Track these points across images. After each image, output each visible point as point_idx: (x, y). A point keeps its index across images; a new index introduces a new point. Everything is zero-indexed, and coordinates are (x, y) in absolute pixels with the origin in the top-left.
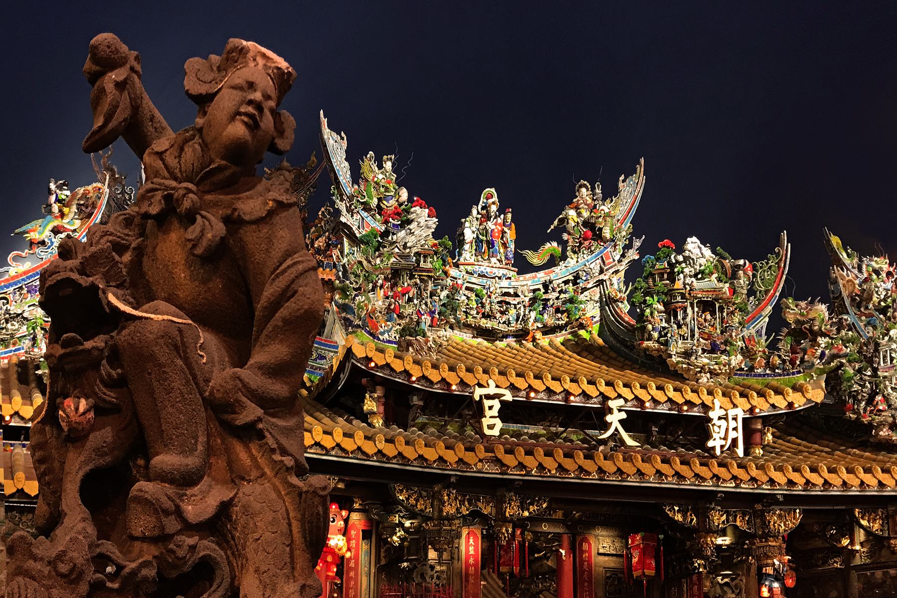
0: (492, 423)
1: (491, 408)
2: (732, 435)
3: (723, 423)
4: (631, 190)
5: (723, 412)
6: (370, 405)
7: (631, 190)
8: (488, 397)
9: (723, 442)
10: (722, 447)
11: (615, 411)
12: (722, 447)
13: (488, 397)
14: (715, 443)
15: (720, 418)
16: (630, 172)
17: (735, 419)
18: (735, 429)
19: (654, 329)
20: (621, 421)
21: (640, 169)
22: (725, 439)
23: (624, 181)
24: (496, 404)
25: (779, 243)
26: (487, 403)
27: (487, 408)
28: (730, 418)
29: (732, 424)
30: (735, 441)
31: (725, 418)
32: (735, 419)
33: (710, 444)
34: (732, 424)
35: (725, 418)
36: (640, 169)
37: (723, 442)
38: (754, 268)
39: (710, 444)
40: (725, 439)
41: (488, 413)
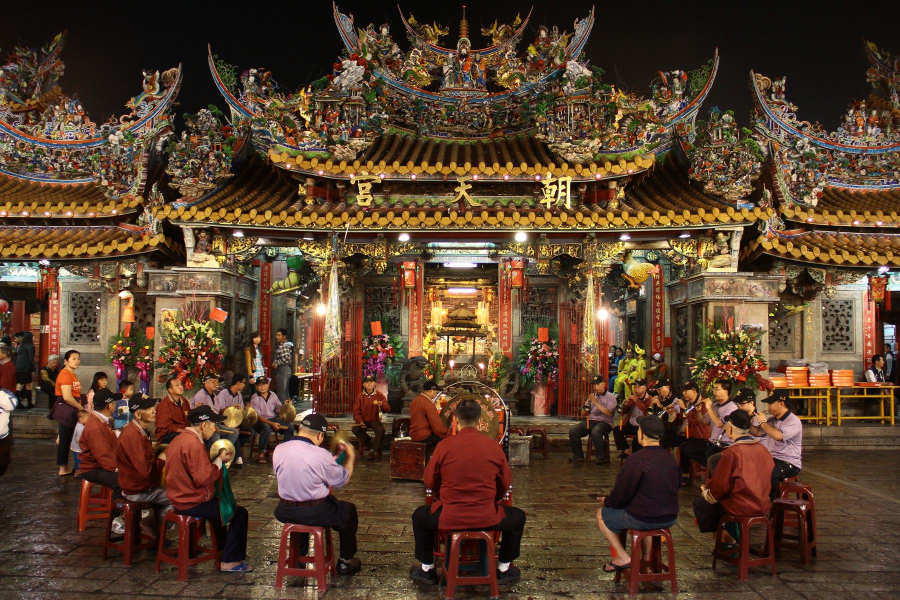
1: (364, 188)
2: (564, 194)
3: (554, 187)
4: (583, 28)
5: (554, 180)
6: (302, 191)
7: (583, 28)
8: (362, 181)
9: (554, 200)
10: (552, 203)
11: (463, 184)
12: (552, 203)
13: (362, 181)
14: (547, 200)
15: (551, 184)
16: (583, 15)
18: (565, 190)
19: (541, 125)
20: (466, 191)
21: (592, 12)
23: (578, 23)
24: (369, 186)
25: (712, 56)
26: (360, 186)
27: (360, 189)
28: (560, 184)
29: (563, 187)
31: (556, 183)
32: (564, 183)
34: (563, 187)
35: (556, 183)
36: (592, 12)
37: (554, 200)
38: (689, 76)
40: (556, 196)
41: (361, 192)
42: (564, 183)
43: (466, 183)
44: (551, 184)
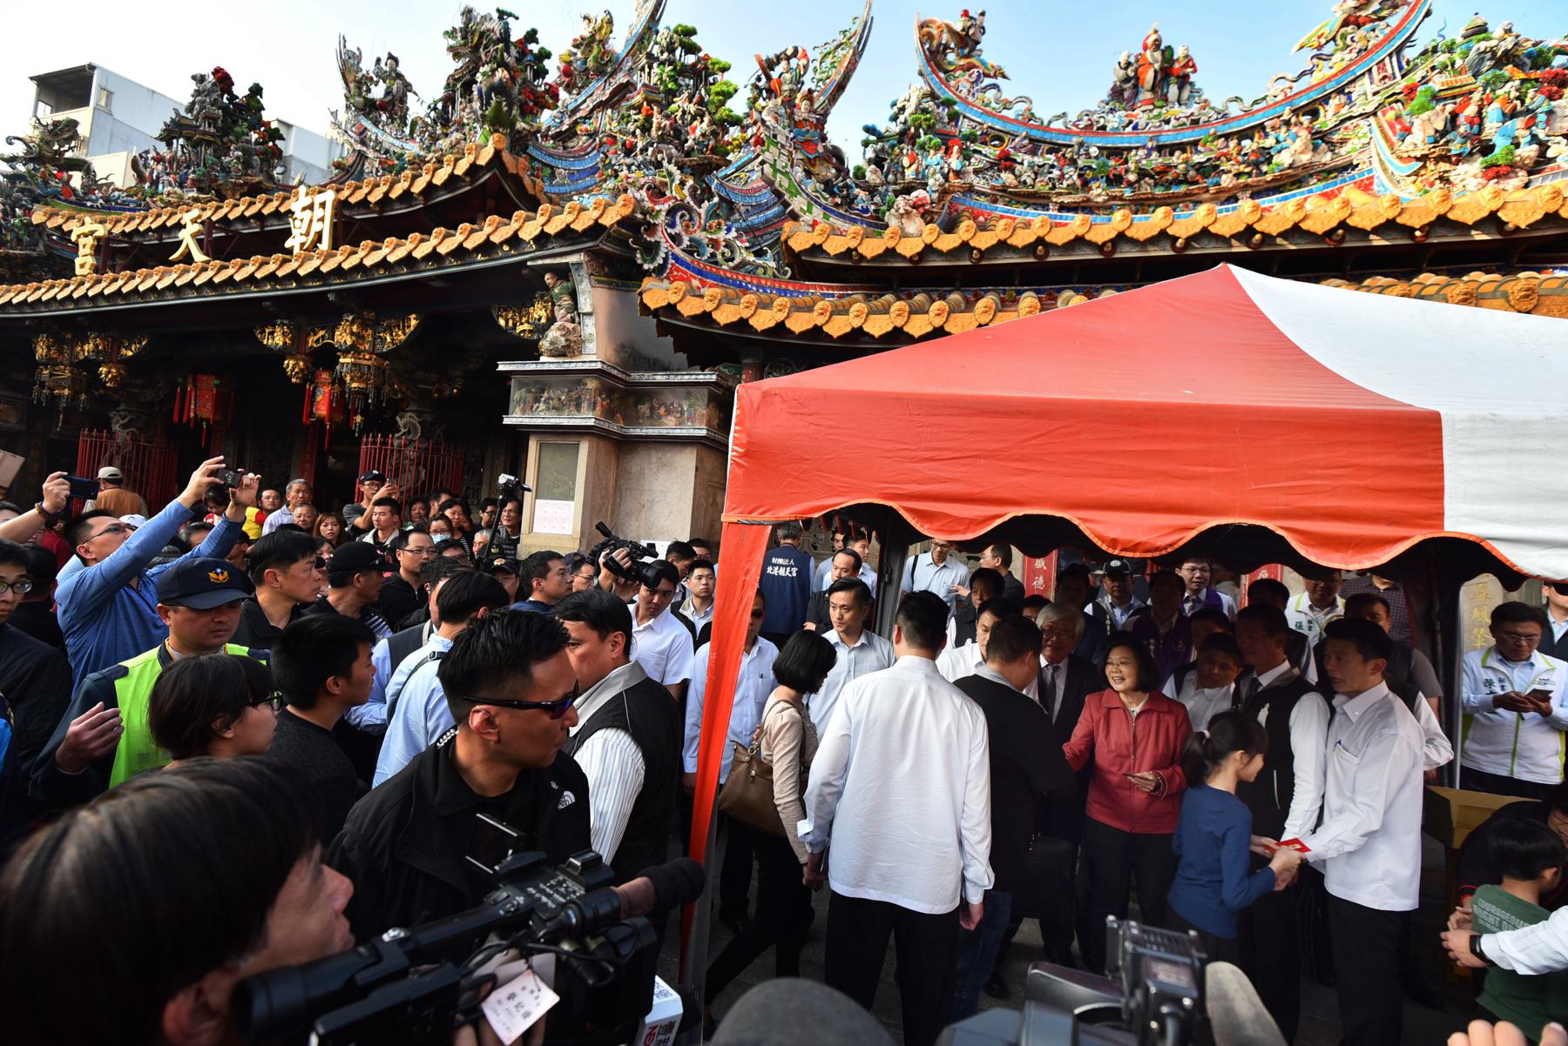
0: (84, 261)
5: (308, 201)
9: (303, 239)
10: (303, 244)
15: (304, 209)
17: (323, 205)
18: (322, 219)
22: (307, 234)
24: (90, 241)
26: (82, 241)
28: (316, 206)
30: (319, 236)
33: (288, 244)
34: (318, 212)
37: (303, 239)
39: (288, 244)
40: (307, 234)
42: (323, 205)
43: (194, 221)
44: (304, 209)
